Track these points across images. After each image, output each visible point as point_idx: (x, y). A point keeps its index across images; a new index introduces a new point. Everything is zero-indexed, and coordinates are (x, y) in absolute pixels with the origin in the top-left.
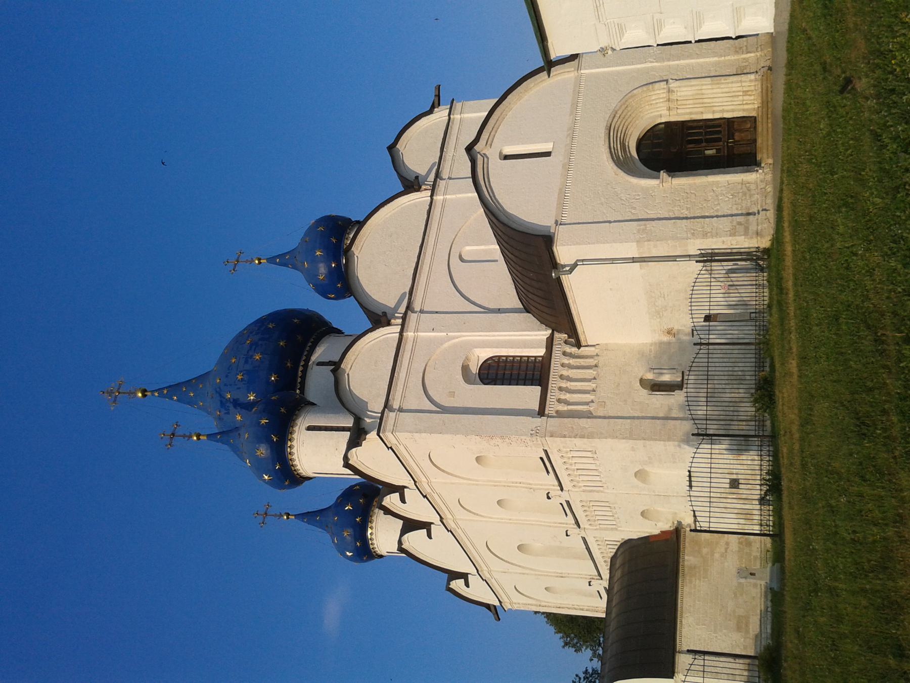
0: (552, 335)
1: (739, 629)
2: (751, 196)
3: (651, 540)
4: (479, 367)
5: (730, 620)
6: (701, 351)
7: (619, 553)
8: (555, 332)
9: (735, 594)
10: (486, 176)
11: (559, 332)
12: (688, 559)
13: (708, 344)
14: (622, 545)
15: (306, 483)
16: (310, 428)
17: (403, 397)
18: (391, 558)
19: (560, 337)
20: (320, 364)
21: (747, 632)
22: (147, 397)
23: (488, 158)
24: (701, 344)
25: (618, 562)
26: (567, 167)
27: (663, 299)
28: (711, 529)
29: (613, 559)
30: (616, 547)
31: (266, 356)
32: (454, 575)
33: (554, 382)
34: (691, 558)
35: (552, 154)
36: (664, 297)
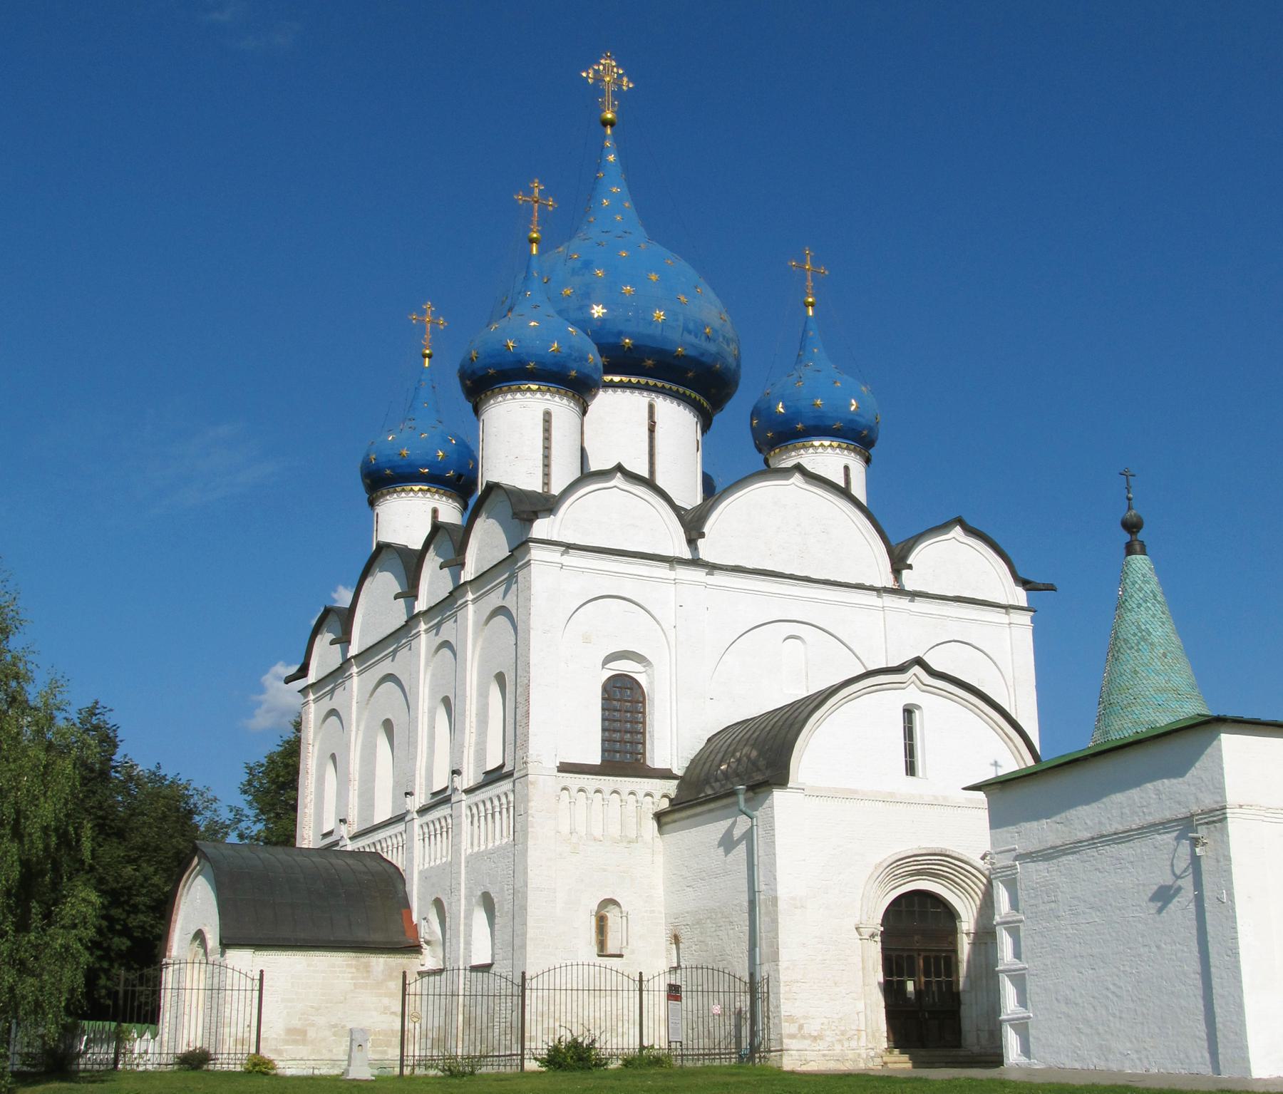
0: (675, 777)
1: (290, 1031)
2: (839, 1041)
3: (404, 911)
4: (628, 674)
5: (300, 1019)
6: (631, 982)
7: (384, 864)
8: (676, 782)
9: (335, 1026)
10: (880, 687)
11: (679, 787)
12: (379, 962)
13: (641, 990)
14: (397, 868)
15: (469, 406)
16: (547, 418)
17: (583, 570)
18: (370, 524)
19: (671, 787)
20: (651, 408)
21: (287, 1042)
22: (602, 127)
23: (904, 689)
24: (641, 981)
25: (372, 864)
26: (890, 800)
27: (713, 929)
28: (407, 996)
29: (377, 856)
30: (394, 862)
31: (660, 329)
32: (347, 616)
33: (608, 782)
34: (381, 967)
35: (910, 778)
36: (716, 931)
